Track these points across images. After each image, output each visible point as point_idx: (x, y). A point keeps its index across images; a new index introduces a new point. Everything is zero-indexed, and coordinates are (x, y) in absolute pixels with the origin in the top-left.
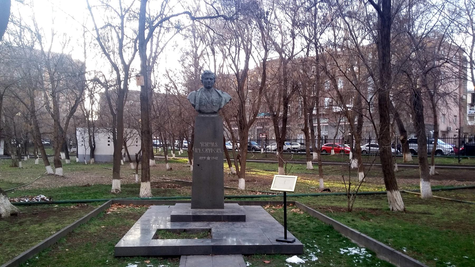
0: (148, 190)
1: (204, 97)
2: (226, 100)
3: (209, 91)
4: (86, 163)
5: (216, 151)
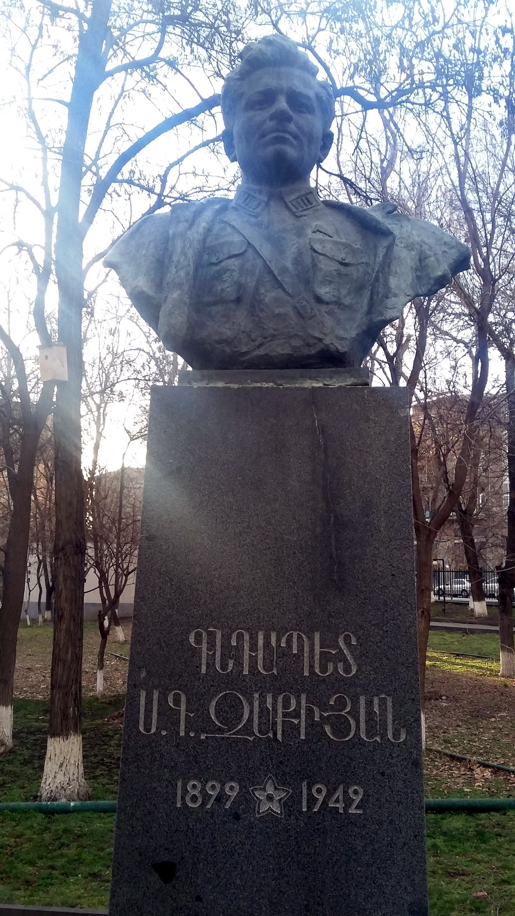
0: (72, 769)
1: (236, 238)
2: (422, 259)
3: (281, 198)
4: (29, 623)
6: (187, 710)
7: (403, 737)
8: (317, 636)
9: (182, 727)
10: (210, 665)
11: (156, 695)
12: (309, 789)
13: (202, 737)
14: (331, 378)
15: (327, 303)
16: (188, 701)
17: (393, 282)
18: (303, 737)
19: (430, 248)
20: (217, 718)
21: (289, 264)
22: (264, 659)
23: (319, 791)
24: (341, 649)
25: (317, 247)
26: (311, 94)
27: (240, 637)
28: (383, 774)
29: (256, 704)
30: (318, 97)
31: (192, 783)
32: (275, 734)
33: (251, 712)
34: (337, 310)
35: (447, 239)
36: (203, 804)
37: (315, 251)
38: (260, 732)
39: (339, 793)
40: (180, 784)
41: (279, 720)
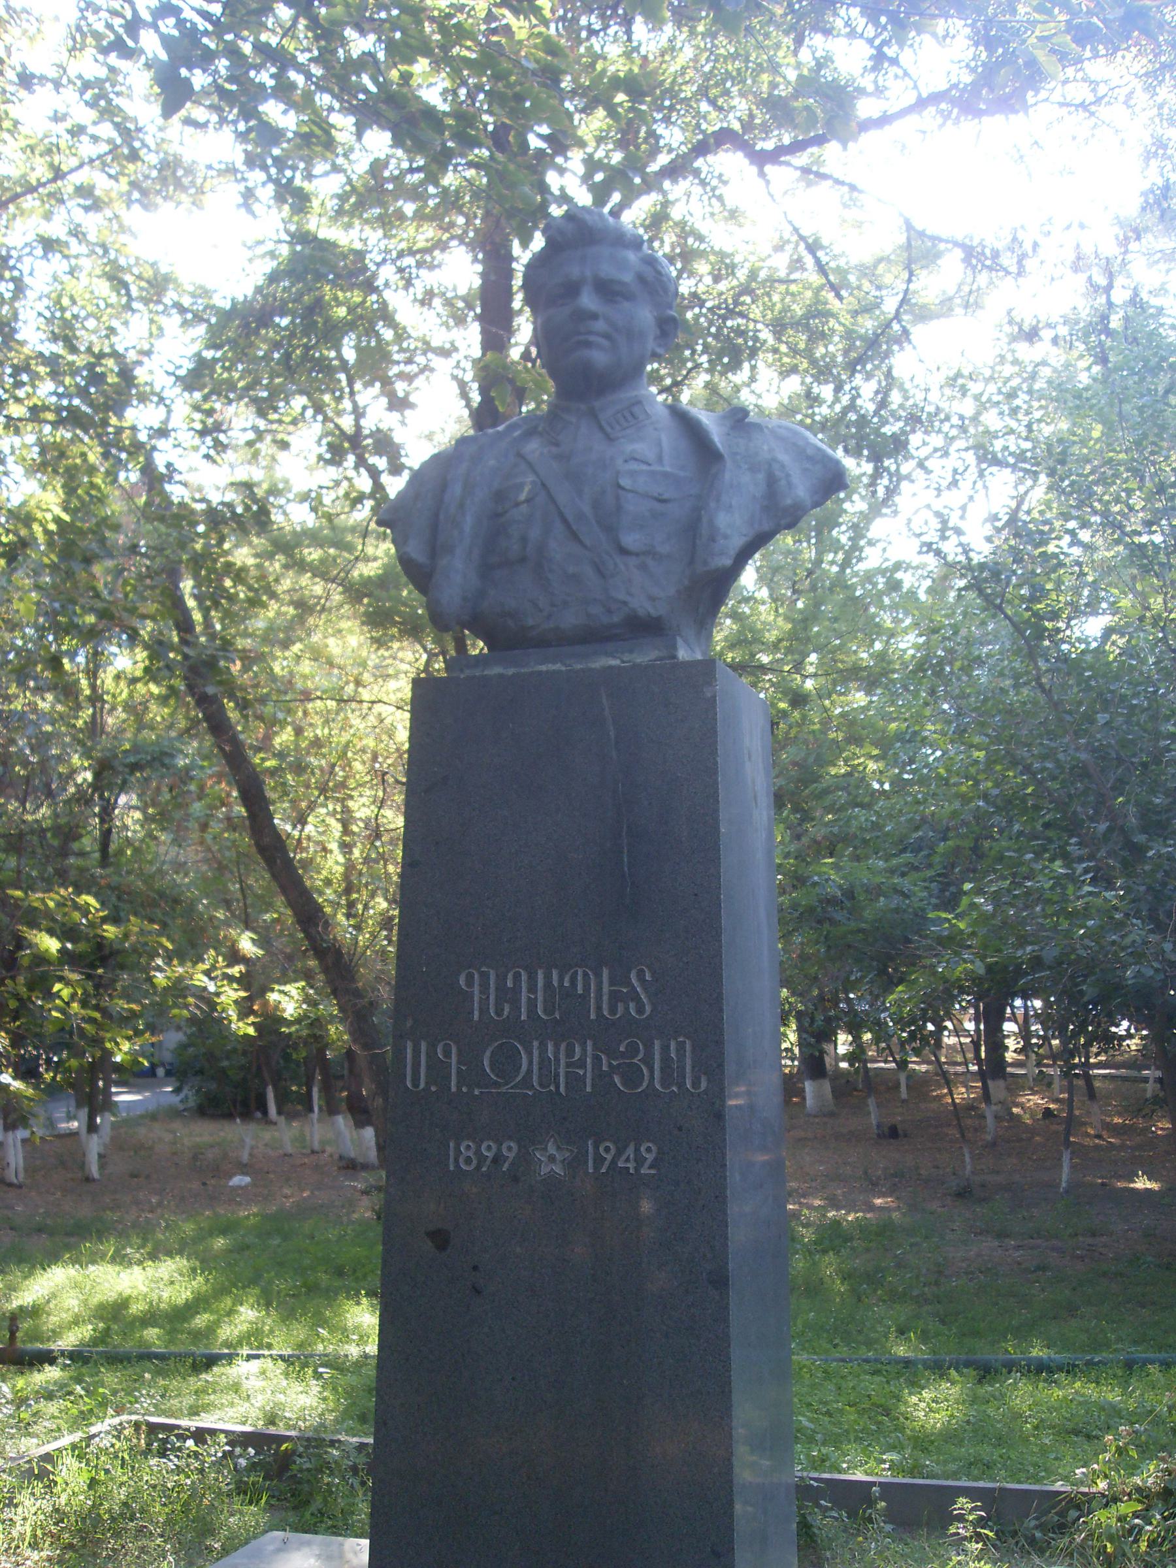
5: (632, 1076)
6: (459, 1062)
7: (704, 1085)
8: (605, 973)
9: (454, 1083)
10: (484, 1010)
11: (423, 1046)
12: (596, 1148)
13: (477, 1092)
14: (631, 651)
15: (637, 555)
16: (460, 1053)
17: (722, 520)
18: (589, 1089)
19: (783, 466)
20: (492, 1070)
21: (587, 509)
22: (545, 1001)
23: (607, 1150)
24: (634, 988)
25: (625, 482)
26: (628, 278)
27: (517, 977)
28: (680, 1129)
29: (536, 1053)
30: (641, 279)
31: (466, 1143)
32: (558, 1087)
33: (531, 1063)
34: (650, 562)
35: (810, 452)
36: (478, 1167)
37: (623, 489)
38: (541, 1085)
39: (630, 1151)
40: (452, 1145)
41: (562, 1071)
